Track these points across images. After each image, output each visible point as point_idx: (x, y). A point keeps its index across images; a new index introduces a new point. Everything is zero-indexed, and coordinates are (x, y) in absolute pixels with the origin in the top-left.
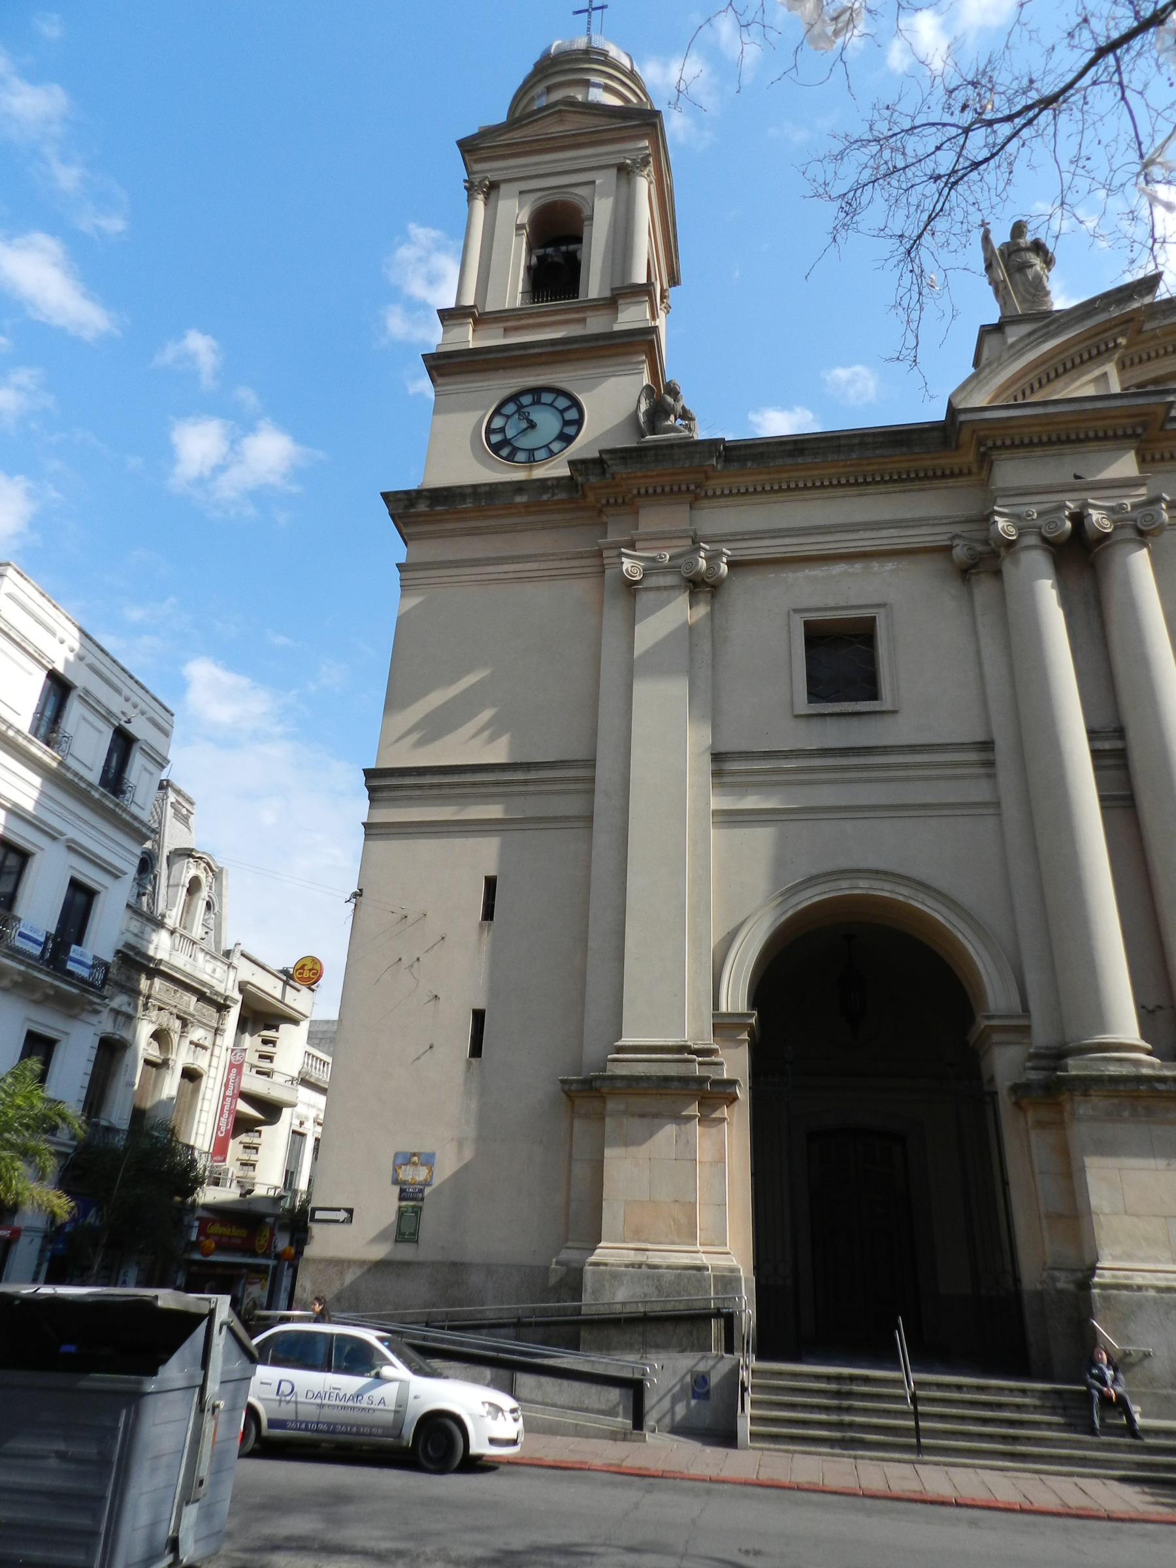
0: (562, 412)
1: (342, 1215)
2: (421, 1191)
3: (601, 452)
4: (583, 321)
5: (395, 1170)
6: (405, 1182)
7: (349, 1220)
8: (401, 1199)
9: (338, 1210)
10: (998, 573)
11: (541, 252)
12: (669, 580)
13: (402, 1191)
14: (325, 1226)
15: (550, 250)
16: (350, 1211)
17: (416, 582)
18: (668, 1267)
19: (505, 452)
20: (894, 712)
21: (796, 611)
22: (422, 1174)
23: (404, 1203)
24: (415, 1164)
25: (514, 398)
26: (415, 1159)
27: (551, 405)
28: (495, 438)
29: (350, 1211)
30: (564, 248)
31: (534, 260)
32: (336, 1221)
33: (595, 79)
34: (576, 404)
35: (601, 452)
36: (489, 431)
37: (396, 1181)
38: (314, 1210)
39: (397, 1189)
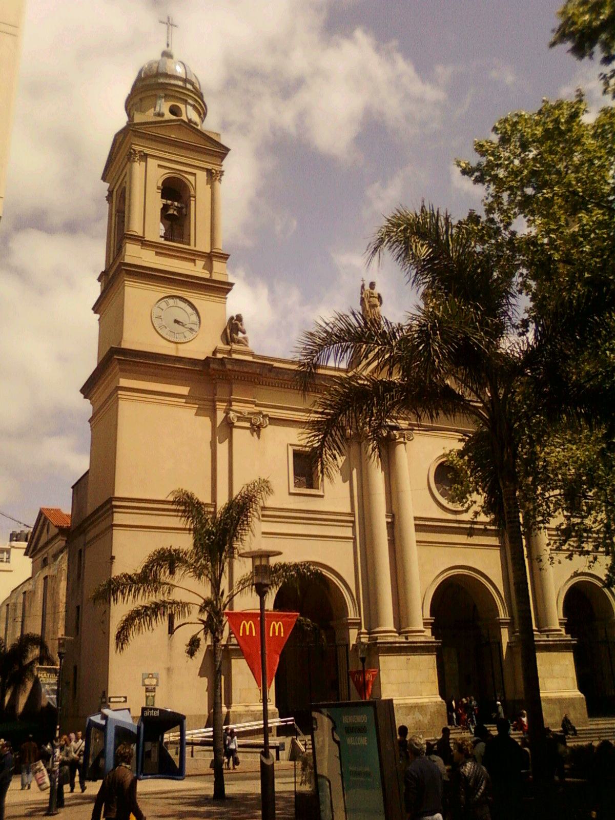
1: (123, 699)
2: (154, 688)
4: (194, 261)
5: (143, 681)
6: (148, 685)
7: (125, 701)
8: (146, 692)
9: (121, 697)
10: (360, 444)
13: (147, 689)
14: (115, 704)
15: (169, 202)
16: (125, 698)
17: (126, 397)
18: (258, 711)
20: (322, 496)
21: (291, 445)
22: (154, 682)
23: (148, 694)
24: (151, 678)
26: (151, 676)
29: (125, 698)
32: (120, 702)
37: (144, 685)
38: (110, 698)
39: (144, 688)
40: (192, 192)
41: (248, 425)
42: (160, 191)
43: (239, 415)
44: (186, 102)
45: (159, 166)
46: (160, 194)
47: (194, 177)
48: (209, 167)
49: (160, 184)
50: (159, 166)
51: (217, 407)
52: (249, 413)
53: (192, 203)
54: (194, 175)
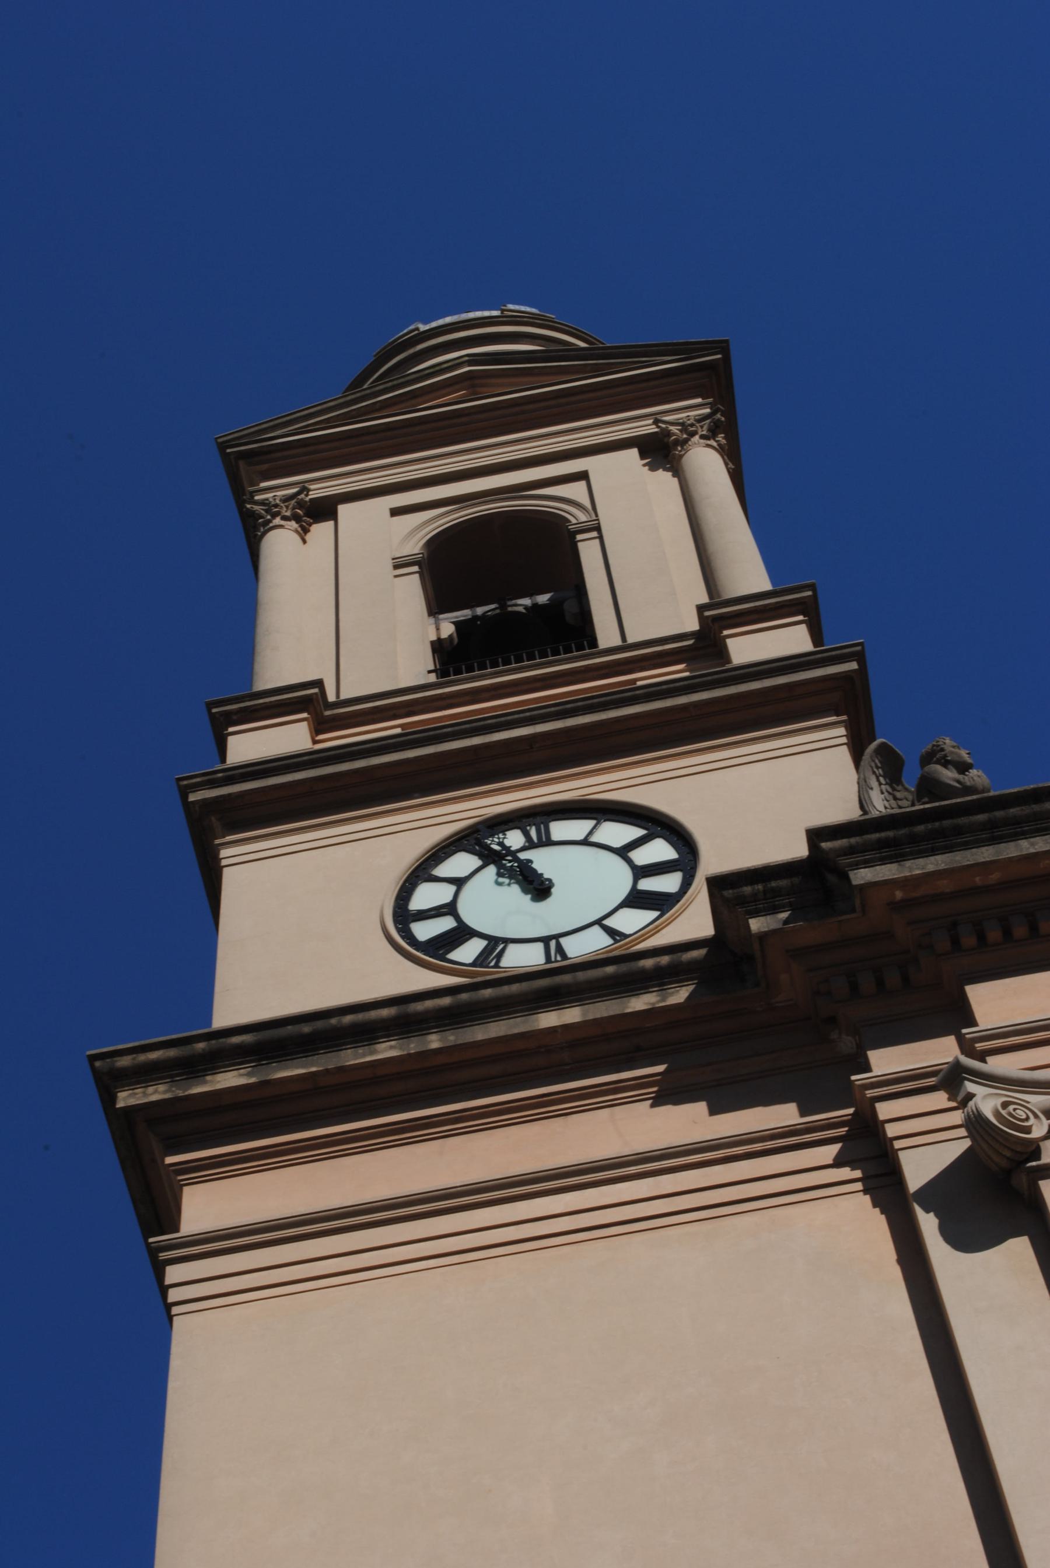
0: (623, 852)
3: (815, 836)
11: (464, 614)
19: (467, 952)
27: (585, 842)
31: (448, 629)
35: (815, 836)
36: (404, 916)
45: (395, 512)
50: (395, 512)
51: (891, 1130)
53: (588, 552)
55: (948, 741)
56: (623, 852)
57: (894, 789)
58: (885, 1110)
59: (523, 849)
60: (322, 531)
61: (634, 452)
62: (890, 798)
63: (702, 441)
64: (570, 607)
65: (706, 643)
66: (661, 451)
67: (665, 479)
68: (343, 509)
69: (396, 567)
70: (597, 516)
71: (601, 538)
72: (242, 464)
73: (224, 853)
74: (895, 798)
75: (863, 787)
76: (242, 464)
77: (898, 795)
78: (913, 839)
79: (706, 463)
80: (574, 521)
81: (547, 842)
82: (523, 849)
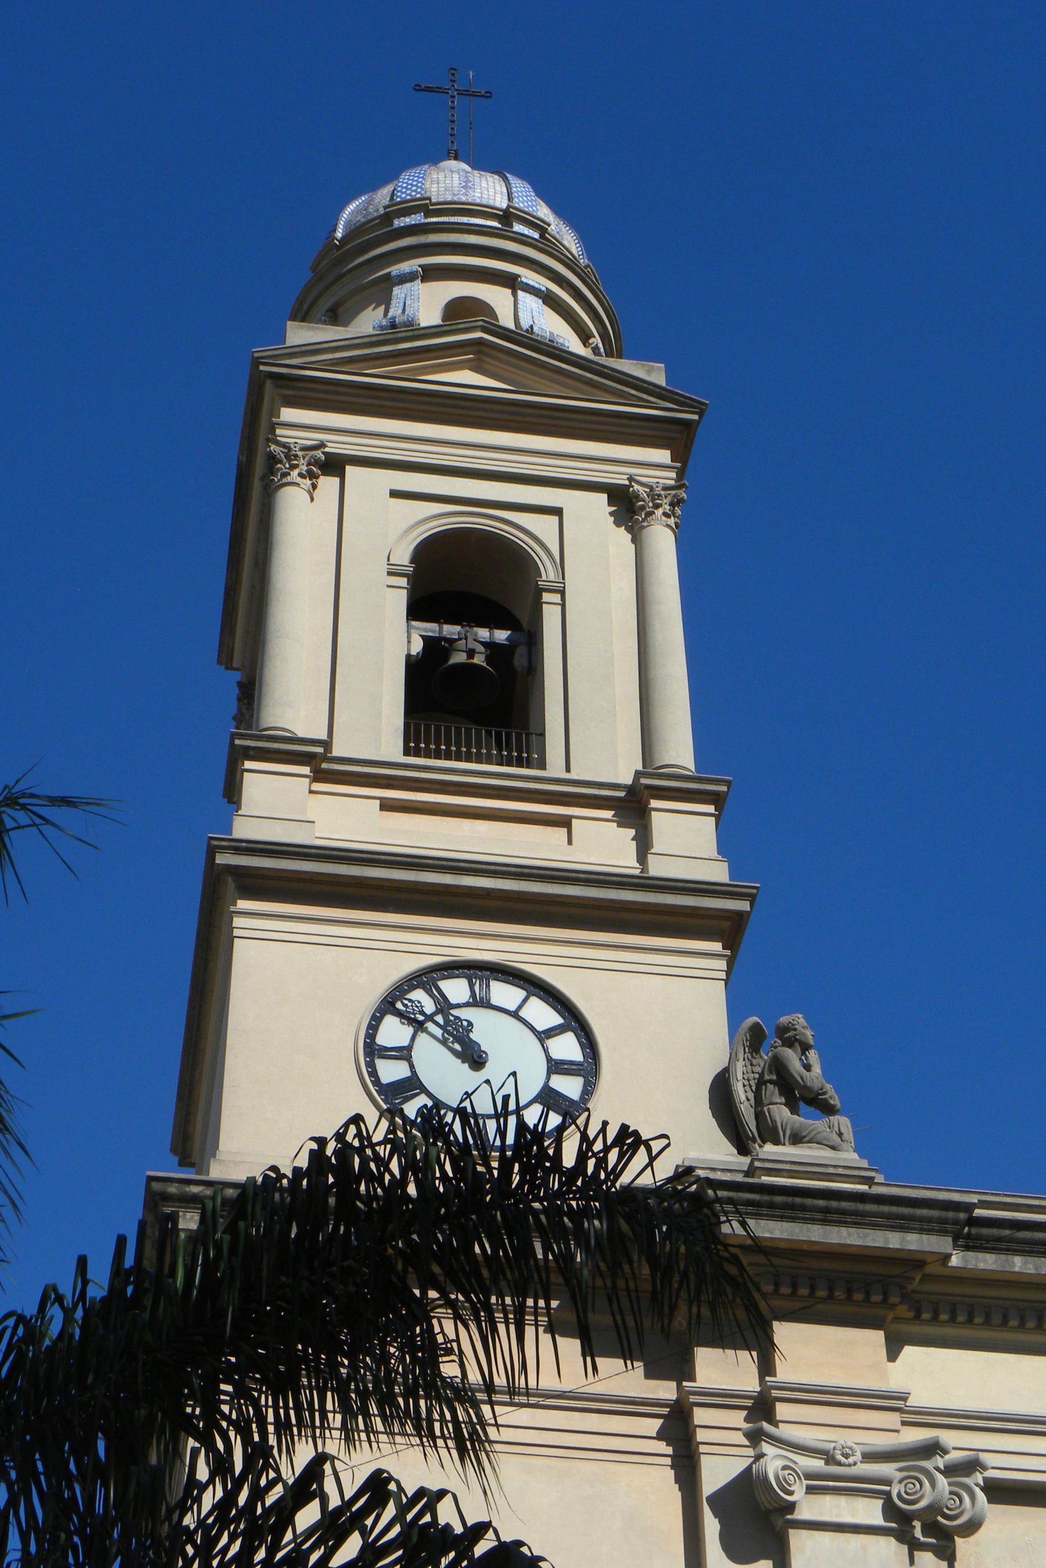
0: (544, 1036)
4: (565, 822)
11: (431, 628)
12: (869, 1511)
15: (451, 630)
25: (426, 978)
27: (515, 1015)
28: (391, 1071)
30: (483, 633)
31: (417, 646)
33: (529, 277)
34: (574, 1020)
36: (373, 1051)
40: (548, 573)
41: (870, 1512)
42: (403, 582)
43: (817, 1464)
44: (511, 282)
45: (395, 494)
46: (403, 595)
47: (557, 518)
48: (618, 477)
49: (403, 557)
50: (395, 494)
51: (701, 1435)
52: (870, 1457)
53: (551, 617)
54: (558, 512)
55: (802, 1020)
56: (544, 1036)
57: (753, 1057)
58: (700, 1416)
59: (467, 1005)
60: (328, 484)
61: (604, 497)
62: (748, 1063)
63: (664, 518)
64: (519, 660)
65: (632, 806)
66: (627, 506)
67: (622, 536)
68: (351, 472)
69: (390, 574)
70: (563, 578)
71: (563, 606)
72: (269, 383)
73: (238, 922)
74: (752, 1065)
75: (733, 1058)
76: (269, 383)
77: (754, 1062)
78: (771, 1205)
79: (662, 540)
80: (544, 578)
81: (484, 1003)
82: (467, 1005)
